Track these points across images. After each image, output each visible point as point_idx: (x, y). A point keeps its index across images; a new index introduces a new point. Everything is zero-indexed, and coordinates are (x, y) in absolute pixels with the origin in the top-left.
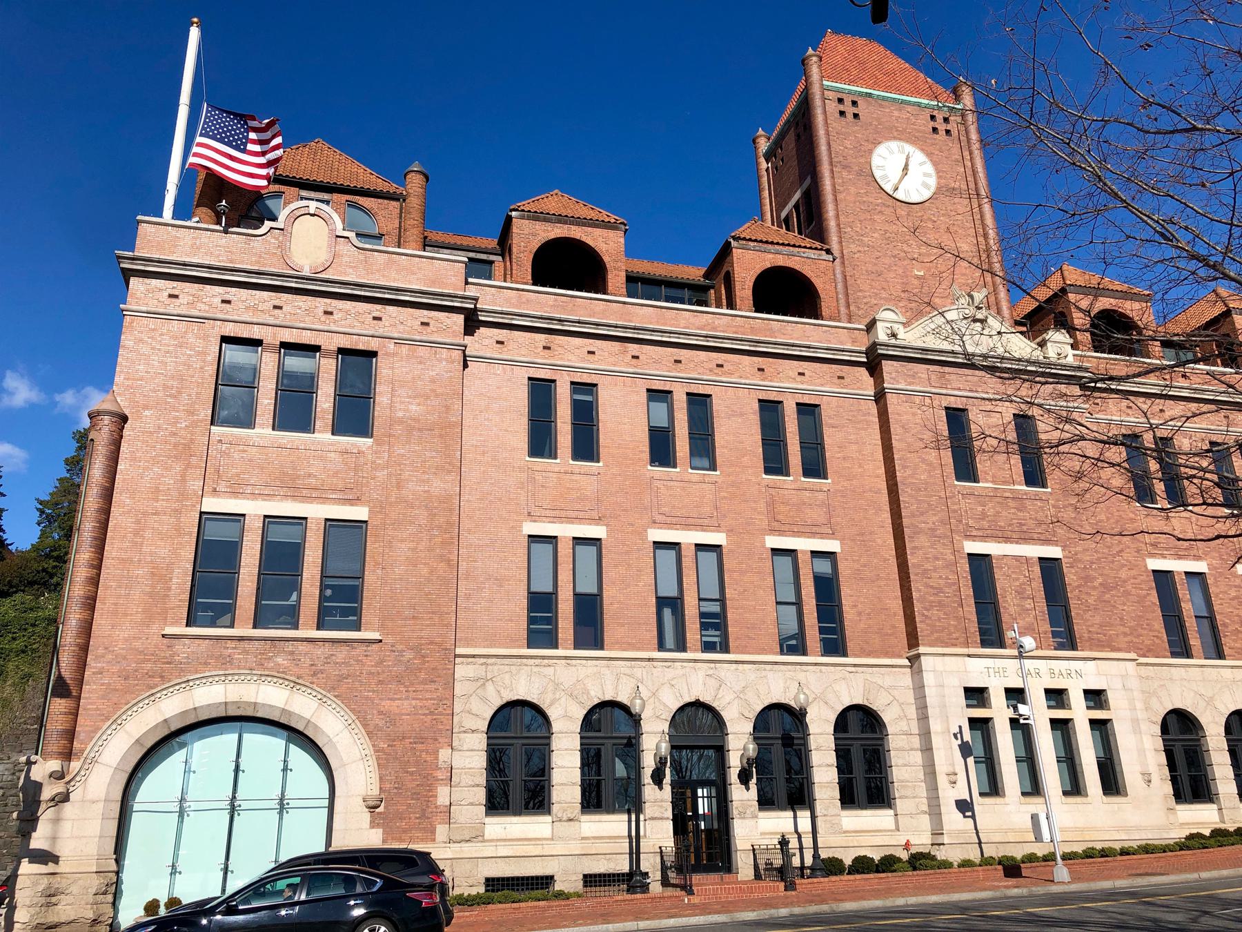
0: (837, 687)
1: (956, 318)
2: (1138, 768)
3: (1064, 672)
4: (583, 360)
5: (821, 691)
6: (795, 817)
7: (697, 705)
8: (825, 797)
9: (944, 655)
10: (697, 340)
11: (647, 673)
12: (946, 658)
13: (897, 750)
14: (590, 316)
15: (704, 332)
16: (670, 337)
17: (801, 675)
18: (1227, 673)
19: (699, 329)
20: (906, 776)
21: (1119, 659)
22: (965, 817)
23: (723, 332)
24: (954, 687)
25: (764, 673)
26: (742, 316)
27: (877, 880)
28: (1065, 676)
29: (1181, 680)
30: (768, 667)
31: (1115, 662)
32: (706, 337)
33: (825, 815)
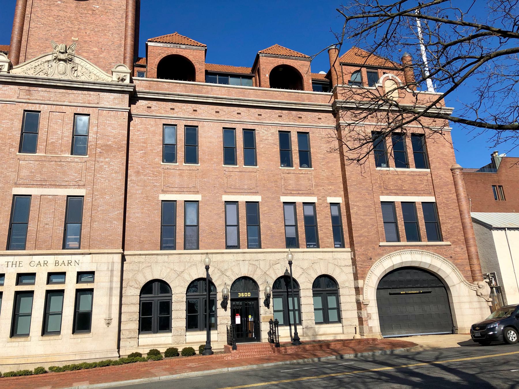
1: (51, 59)
2: (105, 316)
3: (42, 263)
18: (198, 258)
21: (108, 253)
29: (164, 262)
31: (106, 255)
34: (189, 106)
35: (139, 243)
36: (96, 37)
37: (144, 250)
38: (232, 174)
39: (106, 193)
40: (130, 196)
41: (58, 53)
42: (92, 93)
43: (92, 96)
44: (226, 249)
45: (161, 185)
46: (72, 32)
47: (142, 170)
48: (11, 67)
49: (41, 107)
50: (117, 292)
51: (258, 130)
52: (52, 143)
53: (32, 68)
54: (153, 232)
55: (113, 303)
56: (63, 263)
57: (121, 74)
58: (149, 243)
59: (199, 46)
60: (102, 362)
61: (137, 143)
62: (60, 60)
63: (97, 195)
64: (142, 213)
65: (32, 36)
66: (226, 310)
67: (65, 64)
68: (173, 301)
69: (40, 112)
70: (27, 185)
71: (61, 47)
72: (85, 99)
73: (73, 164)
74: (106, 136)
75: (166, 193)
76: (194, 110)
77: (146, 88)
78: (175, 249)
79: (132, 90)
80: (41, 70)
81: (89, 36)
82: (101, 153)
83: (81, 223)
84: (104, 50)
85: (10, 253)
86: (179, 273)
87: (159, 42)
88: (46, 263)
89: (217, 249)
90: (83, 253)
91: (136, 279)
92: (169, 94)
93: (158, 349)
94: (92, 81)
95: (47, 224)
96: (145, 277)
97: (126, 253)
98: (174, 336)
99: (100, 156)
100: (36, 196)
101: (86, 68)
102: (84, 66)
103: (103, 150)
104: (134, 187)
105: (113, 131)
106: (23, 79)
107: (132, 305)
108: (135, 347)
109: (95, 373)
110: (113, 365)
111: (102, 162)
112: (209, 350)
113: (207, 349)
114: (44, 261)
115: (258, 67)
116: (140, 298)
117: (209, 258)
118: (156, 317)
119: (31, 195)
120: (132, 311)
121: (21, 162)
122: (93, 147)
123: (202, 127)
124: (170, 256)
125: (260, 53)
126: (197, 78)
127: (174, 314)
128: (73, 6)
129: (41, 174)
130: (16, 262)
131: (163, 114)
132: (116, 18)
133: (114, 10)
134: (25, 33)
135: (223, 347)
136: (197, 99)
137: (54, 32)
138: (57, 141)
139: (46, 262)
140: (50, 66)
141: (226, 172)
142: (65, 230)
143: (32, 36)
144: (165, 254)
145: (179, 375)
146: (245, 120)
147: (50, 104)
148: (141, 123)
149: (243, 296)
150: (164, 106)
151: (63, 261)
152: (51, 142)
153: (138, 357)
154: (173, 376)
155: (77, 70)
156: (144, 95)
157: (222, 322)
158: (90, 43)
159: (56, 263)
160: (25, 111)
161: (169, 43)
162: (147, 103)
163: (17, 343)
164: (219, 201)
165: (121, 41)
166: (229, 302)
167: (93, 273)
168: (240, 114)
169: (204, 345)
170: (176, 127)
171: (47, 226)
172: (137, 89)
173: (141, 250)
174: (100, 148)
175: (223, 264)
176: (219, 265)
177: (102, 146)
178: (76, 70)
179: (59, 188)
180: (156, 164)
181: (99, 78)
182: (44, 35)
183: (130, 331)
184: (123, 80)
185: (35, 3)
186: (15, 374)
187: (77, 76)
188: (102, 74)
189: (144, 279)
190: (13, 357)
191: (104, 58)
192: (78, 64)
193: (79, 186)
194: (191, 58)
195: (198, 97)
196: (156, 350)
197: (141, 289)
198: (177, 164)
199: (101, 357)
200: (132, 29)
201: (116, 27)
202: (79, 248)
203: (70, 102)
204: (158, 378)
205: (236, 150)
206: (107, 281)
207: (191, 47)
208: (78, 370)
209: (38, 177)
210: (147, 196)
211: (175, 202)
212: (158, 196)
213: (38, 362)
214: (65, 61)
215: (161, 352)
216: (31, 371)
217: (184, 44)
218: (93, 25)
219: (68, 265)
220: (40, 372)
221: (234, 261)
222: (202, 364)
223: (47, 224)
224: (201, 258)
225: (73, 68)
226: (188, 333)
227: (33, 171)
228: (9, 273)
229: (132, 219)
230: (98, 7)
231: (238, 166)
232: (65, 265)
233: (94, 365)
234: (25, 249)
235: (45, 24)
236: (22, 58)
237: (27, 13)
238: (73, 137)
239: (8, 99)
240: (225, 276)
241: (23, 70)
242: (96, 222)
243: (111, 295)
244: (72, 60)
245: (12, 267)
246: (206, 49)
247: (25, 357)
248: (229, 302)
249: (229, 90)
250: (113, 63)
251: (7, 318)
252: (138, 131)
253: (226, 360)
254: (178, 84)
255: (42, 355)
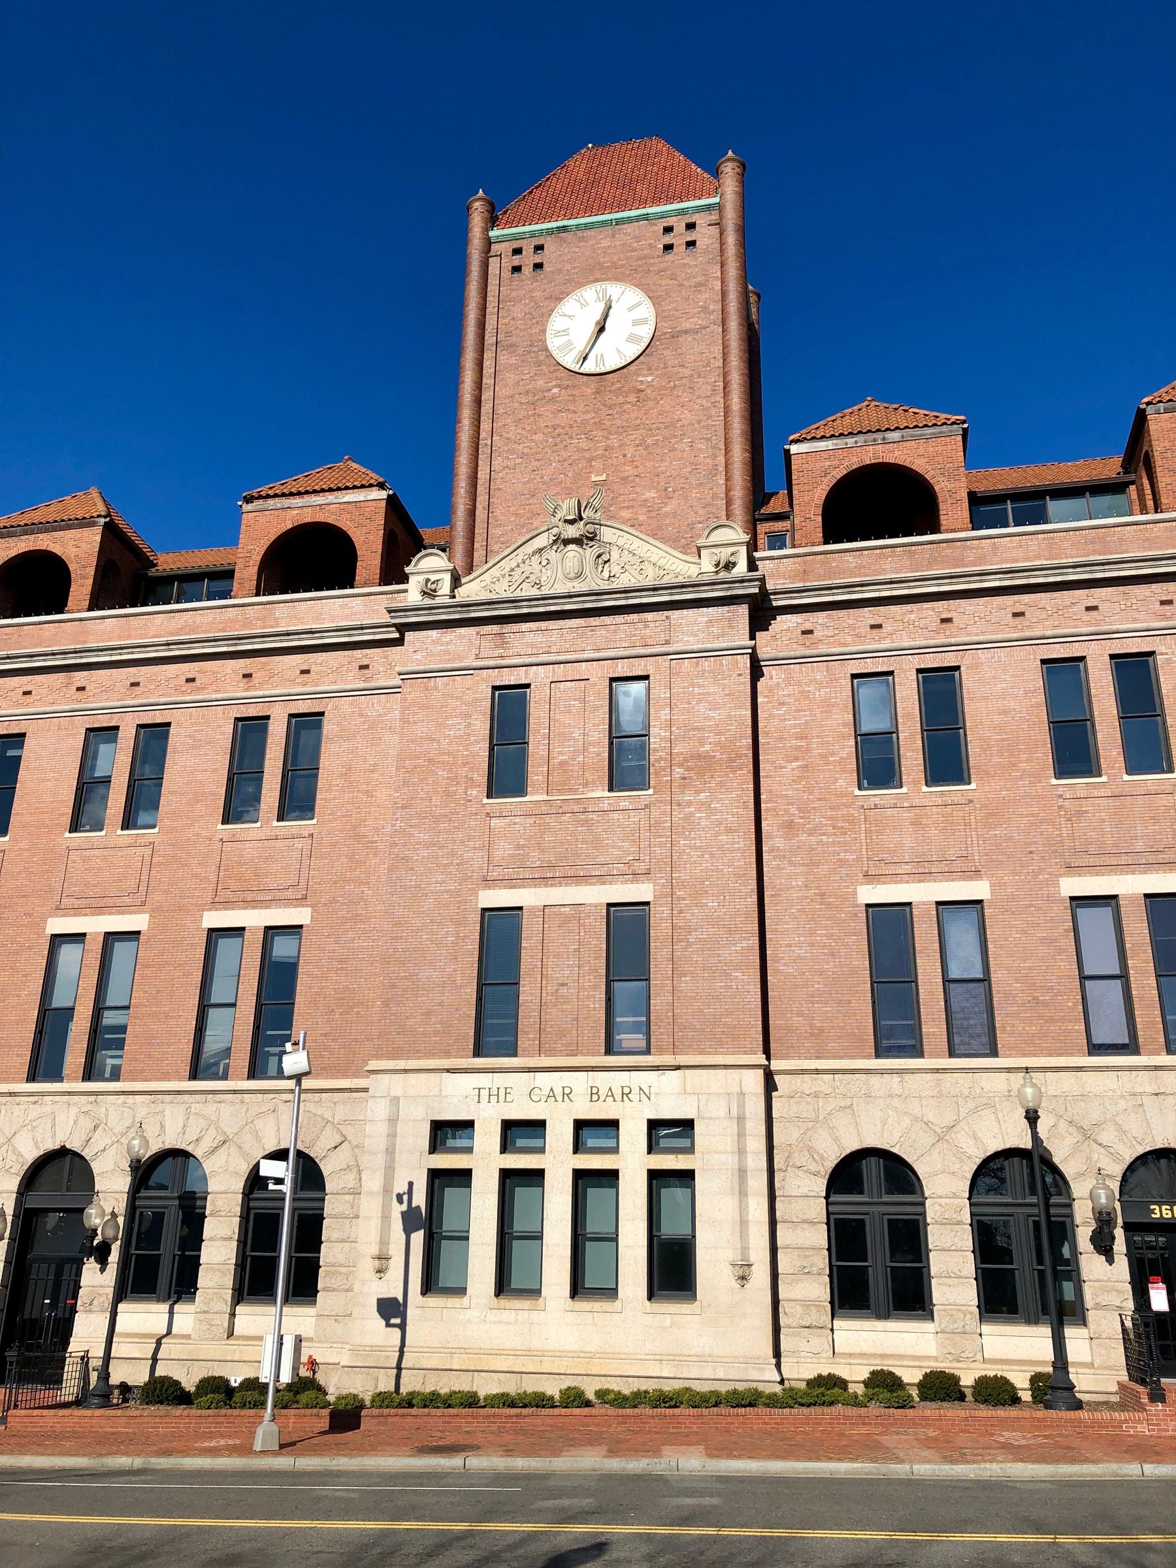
0: (259, 1124)
2: (731, 1254)
3: (558, 1092)
4: (17, 704)
5: (235, 1131)
6: (171, 1313)
7: (63, 1153)
8: (211, 1284)
9: (406, 1071)
10: (156, 651)
11: (6, 1111)
12: (411, 1075)
13: (334, 1217)
14: (36, 646)
15: (163, 639)
16: (121, 654)
17: (210, 1108)
18: (999, 1083)
19: (172, 634)
20: (341, 1258)
21: (726, 1067)
22: (388, 1325)
23: (205, 632)
24: (414, 1121)
25: (160, 1107)
26: (234, 606)
27: (124, 1420)
28: (559, 1098)
29: (891, 1096)
30: (168, 1098)
32: (168, 644)
33: (205, 1312)
34: (927, 609)
35: (812, 1035)
36: (650, 460)
37: (828, 1058)
38: (1087, 806)
39: (706, 892)
40: (772, 896)
41: (561, 524)
42: (649, 616)
43: (652, 625)
44: (1090, 1054)
45: (859, 859)
46: (590, 460)
47: (802, 818)
48: (456, 582)
49: (531, 674)
50: (758, 1183)
51: (1166, 654)
52: (563, 764)
53: (504, 576)
54: (849, 1002)
55: (751, 1217)
56: (610, 1094)
57: (723, 549)
58: (840, 1037)
59: (944, 424)
60: (735, 1392)
61: (781, 739)
62: (567, 542)
63: (684, 899)
64: (812, 945)
65: (498, 493)
66: (1110, 1261)
67: (580, 550)
68: (929, 1220)
69: (528, 686)
70: (511, 883)
71: (567, 508)
72: (635, 635)
73: (616, 816)
74: (694, 729)
75: (879, 882)
76: (944, 621)
77: (793, 578)
78: (921, 1055)
79: (756, 590)
80: (524, 576)
81: (633, 461)
82: (684, 778)
83: (648, 980)
84: (674, 491)
85: (483, 1064)
86: (939, 1131)
87: (823, 437)
88: (567, 1095)
89: (1060, 1055)
90: (658, 1066)
91: (811, 1147)
92: (862, 585)
93: (898, 1372)
94: (649, 582)
95: (562, 985)
96: (836, 1139)
97: (775, 1065)
98: (941, 1332)
99: (683, 787)
100: (533, 909)
101: (630, 552)
102: (626, 546)
103: (688, 769)
104: (783, 869)
105: (712, 713)
106: (487, 607)
107: (806, 1226)
108: (825, 1355)
109: (718, 1423)
110: (767, 1405)
111: (690, 804)
112: (1066, 1394)
113: (1059, 1388)
114: (563, 1088)
115: (1145, 448)
116: (828, 1204)
117: (1034, 1085)
118: (879, 1265)
119: (520, 908)
120: (807, 1243)
121: (494, 822)
122: (663, 763)
123: (975, 666)
124: (907, 1077)
125: (1148, 404)
126: (943, 522)
127: (937, 1263)
128: (589, 391)
129: (543, 851)
130: (498, 1089)
131: (848, 645)
132: (699, 397)
133: (692, 376)
134: (481, 489)
135: (1114, 1388)
136: (951, 584)
137: (548, 471)
138: (574, 759)
139: (567, 1091)
140: (546, 562)
141: (1067, 803)
142: (609, 999)
143: (498, 493)
144: (892, 1072)
145: (975, 1466)
146: (1114, 628)
147: (550, 662)
148: (788, 681)
149: (1170, 1216)
150: (851, 622)
151: (610, 1089)
152: (560, 763)
153: (836, 1390)
154: (954, 1467)
155: (609, 560)
156: (791, 598)
157: (1104, 1299)
158: (637, 479)
159: (592, 1094)
160: (495, 688)
161: (850, 433)
162: (800, 621)
163: (513, 1313)
164: (1052, 899)
165: (715, 456)
166: (1119, 1233)
167: (687, 1125)
168: (1095, 608)
169: (1048, 1375)
170: (891, 678)
171: (564, 990)
172: (770, 586)
173: (818, 1058)
174: (680, 765)
175: (1083, 1104)
176: (1069, 1109)
177: (686, 760)
178: (606, 562)
179: (587, 883)
180: (842, 795)
181: (665, 572)
182: (525, 484)
183: (807, 1304)
184: (729, 566)
185: (499, 407)
186: (512, 1401)
187: (610, 577)
188: (673, 560)
189: (835, 1147)
190: (505, 1352)
191: (674, 514)
192: (610, 544)
193: (635, 876)
194: (919, 465)
195: (951, 577)
196: (891, 1373)
197: (827, 1176)
198: (904, 790)
199: (731, 1378)
200: (743, 417)
201: (699, 422)
202: (647, 1052)
203: (599, 650)
204: (907, 1467)
205: (1093, 726)
206: (729, 1148)
207: (918, 432)
208: (670, 1407)
209: (535, 857)
210: (822, 895)
211: (907, 909)
212: (855, 893)
213: (568, 1372)
214: (578, 541)
215: (906, 1380)
216: (552, 1398)
217: (897, 428)
218: (641, 431)
219: (623, 1101)
220: (574, 1401)
221: (1122, 1096)
222: (1045, 1437)
223: (562, 985)
224: (1009, 1085)
225: (599, 556)
226: (986, 1328)
227: (522, 842)
228: (484, 1120)
229: (785, 965)
230: (650, 379)
231: (1104, 779)
232: (615, 1101)
233: (713, 1400)
234: (515, 1055)
235: (527, 455)
236: (479, 554)
237: (483, 435)
238: (611, 744)
239: (455, 665)
240: (1095, 1146)
241: (483, 584)
242: (685, 975)
243: (743, 1193)
244: (596, 536)
245: (489, 1102)
246: (963, 429)
247: (535, 1353)
248: (1119, 1233)
249: (1053, 538)
250: (700, 523)
251: (484, 1241)
252: (780, 704)
253: (1131, 1436)
254: (888, 550)
255: (575, 1352)
